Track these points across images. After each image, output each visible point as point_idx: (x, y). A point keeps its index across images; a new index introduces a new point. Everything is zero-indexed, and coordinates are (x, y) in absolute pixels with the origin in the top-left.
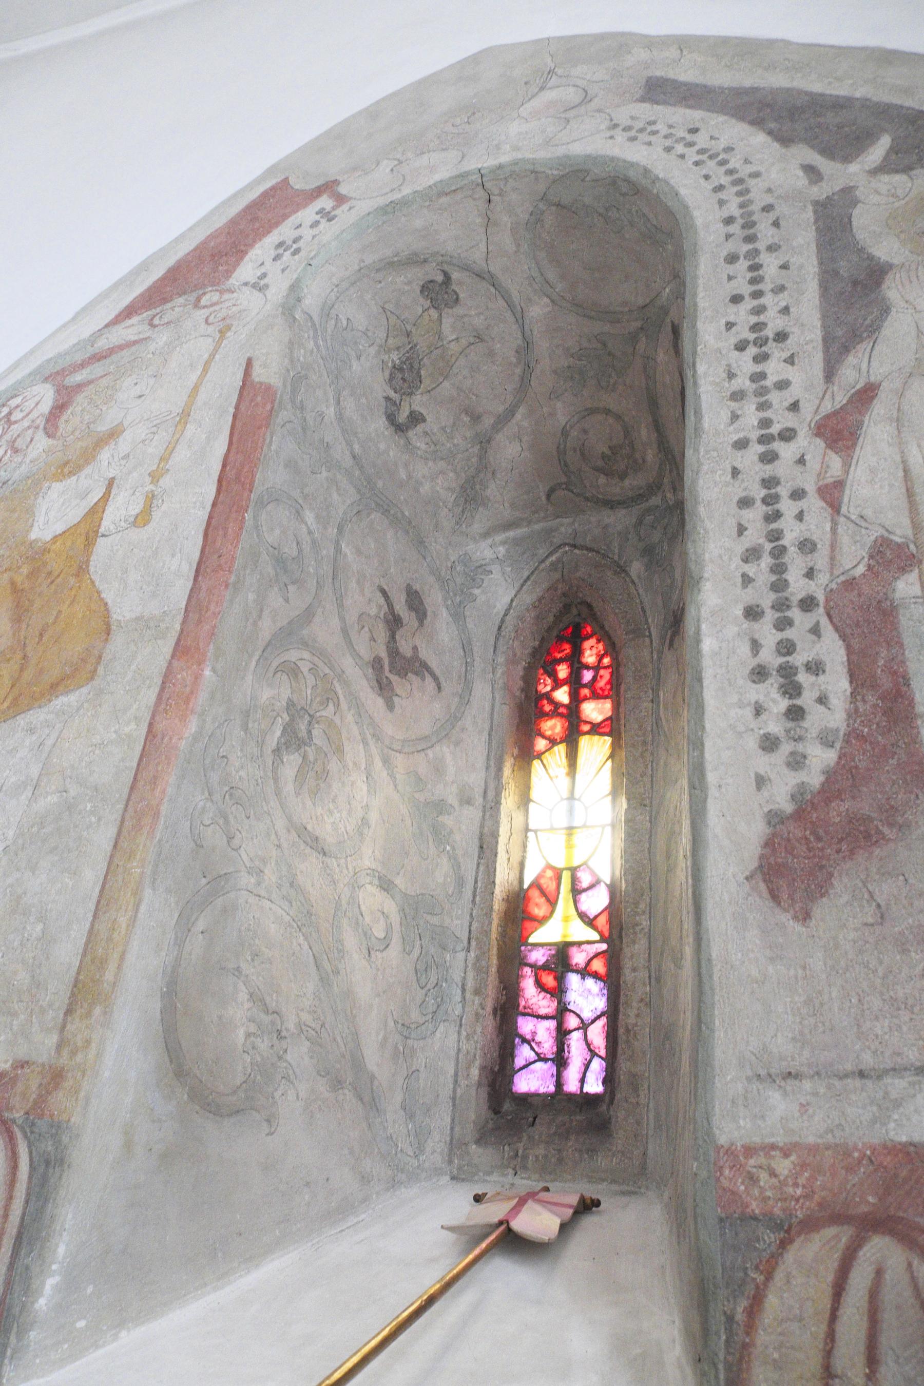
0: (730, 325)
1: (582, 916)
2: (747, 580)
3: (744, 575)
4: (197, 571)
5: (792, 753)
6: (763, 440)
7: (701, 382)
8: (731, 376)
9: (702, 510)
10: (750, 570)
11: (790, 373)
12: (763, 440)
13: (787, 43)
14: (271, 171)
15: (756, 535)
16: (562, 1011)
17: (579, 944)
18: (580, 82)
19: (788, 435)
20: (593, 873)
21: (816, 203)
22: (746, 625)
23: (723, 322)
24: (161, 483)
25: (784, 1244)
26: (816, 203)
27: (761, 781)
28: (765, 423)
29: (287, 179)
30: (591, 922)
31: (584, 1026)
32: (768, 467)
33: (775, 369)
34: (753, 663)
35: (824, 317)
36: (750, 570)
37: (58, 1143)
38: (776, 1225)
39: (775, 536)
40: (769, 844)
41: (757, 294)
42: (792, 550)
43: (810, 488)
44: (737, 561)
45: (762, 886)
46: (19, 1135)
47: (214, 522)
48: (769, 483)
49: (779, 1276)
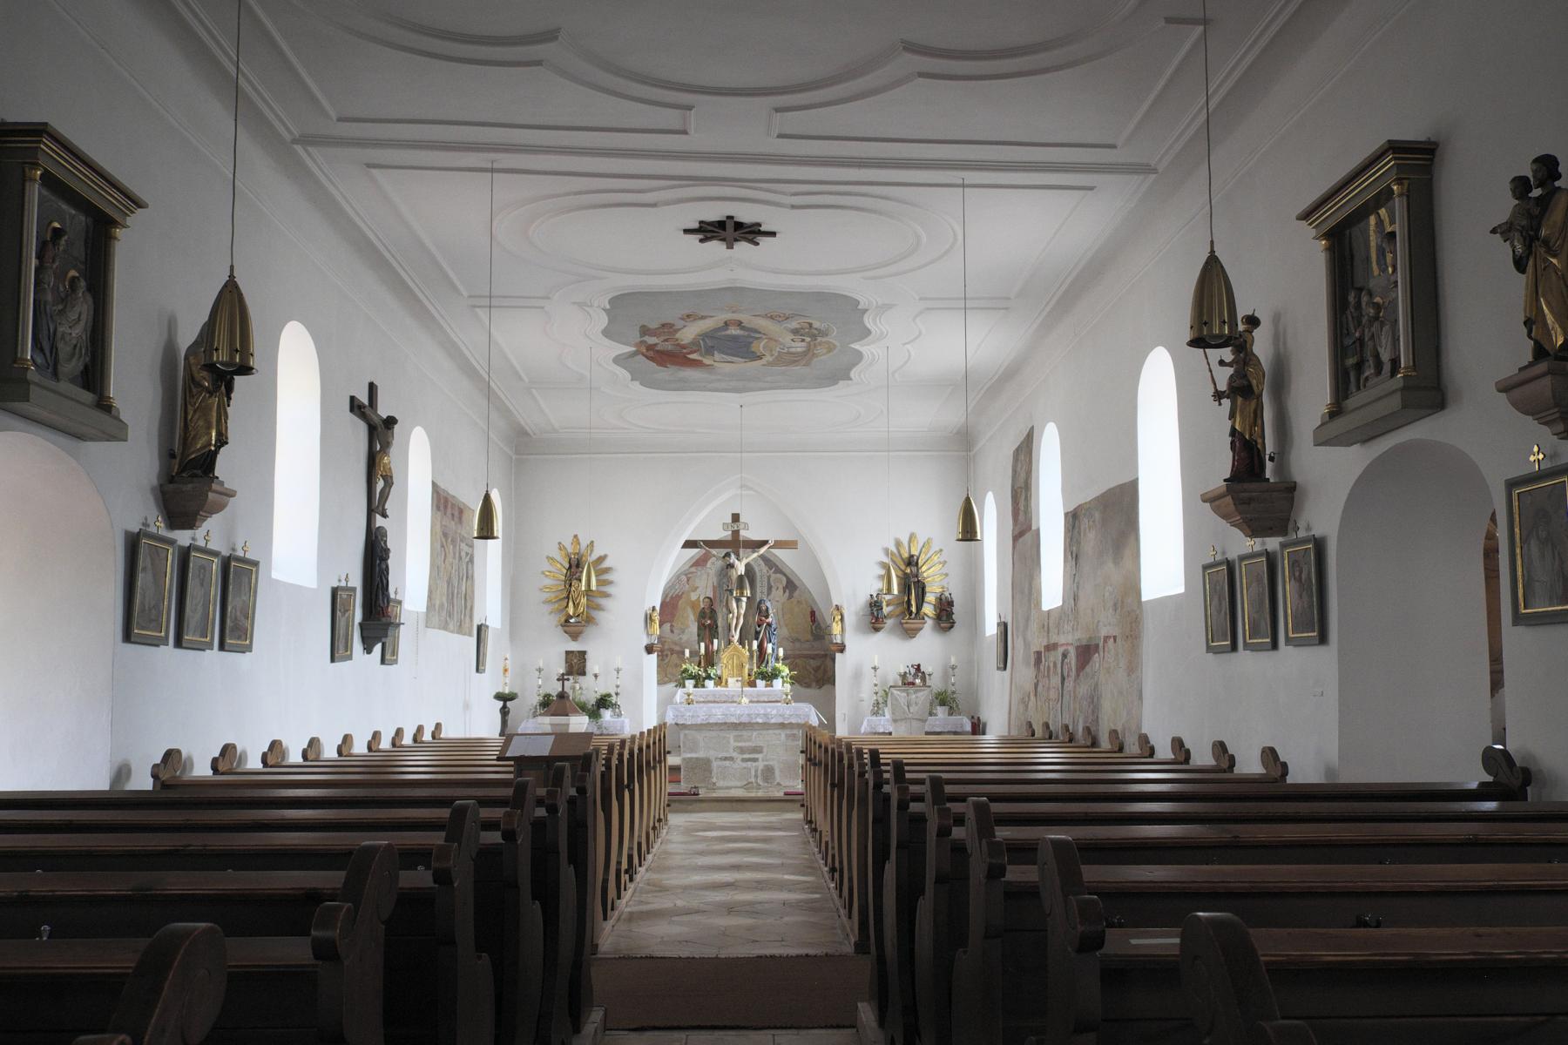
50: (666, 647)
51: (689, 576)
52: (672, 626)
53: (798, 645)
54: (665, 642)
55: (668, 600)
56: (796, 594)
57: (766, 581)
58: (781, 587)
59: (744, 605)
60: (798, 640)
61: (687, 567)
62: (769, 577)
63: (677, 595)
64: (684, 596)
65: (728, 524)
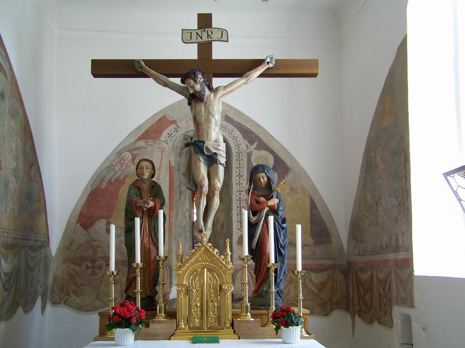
0: (236, 172)
2: (237, 210)
3: (237, 210)
4: (169, 198)
5: (241, 231)
6: (240, 191)
7: (233, 180)
8: (236, 180)
9: (233, 200)
10: (238, 209)
11: (243, 182)
12: (240, 191)
13: (245, 115)
14: (161, 111)
15: (238, 205)
19: (242, 191)
21: (247, 153)
22: (237, 216)
23: (235, 171)
24: (159, 181)
25: (238, 272)
26: (247, 153)
27: (238, 233)
28: (240, 189)
29: (165, 115)
32: (240, 196)
33: (241, 180)
34: (237, 220)
35: (247, 174)
36: (238, 209)
37: (171, 267)
38: (238, 270)
39: (240, 205)
40: (238, 239)
41: (240, 168)
42: (242, 207)
43: (244, 200)
44: (236, 208)
45: (238, 243)
46: (167, 267)
47: (170, 190)
48: (240, 198)
49: (238, 274)
50: (99, 255)
51: (135, 152)
54: (98, 247)
55: (104, 185)
57: (245, 159)
61: (133, 140)
62: (249, 155)
63: (117, 180)
65: (190, 31)
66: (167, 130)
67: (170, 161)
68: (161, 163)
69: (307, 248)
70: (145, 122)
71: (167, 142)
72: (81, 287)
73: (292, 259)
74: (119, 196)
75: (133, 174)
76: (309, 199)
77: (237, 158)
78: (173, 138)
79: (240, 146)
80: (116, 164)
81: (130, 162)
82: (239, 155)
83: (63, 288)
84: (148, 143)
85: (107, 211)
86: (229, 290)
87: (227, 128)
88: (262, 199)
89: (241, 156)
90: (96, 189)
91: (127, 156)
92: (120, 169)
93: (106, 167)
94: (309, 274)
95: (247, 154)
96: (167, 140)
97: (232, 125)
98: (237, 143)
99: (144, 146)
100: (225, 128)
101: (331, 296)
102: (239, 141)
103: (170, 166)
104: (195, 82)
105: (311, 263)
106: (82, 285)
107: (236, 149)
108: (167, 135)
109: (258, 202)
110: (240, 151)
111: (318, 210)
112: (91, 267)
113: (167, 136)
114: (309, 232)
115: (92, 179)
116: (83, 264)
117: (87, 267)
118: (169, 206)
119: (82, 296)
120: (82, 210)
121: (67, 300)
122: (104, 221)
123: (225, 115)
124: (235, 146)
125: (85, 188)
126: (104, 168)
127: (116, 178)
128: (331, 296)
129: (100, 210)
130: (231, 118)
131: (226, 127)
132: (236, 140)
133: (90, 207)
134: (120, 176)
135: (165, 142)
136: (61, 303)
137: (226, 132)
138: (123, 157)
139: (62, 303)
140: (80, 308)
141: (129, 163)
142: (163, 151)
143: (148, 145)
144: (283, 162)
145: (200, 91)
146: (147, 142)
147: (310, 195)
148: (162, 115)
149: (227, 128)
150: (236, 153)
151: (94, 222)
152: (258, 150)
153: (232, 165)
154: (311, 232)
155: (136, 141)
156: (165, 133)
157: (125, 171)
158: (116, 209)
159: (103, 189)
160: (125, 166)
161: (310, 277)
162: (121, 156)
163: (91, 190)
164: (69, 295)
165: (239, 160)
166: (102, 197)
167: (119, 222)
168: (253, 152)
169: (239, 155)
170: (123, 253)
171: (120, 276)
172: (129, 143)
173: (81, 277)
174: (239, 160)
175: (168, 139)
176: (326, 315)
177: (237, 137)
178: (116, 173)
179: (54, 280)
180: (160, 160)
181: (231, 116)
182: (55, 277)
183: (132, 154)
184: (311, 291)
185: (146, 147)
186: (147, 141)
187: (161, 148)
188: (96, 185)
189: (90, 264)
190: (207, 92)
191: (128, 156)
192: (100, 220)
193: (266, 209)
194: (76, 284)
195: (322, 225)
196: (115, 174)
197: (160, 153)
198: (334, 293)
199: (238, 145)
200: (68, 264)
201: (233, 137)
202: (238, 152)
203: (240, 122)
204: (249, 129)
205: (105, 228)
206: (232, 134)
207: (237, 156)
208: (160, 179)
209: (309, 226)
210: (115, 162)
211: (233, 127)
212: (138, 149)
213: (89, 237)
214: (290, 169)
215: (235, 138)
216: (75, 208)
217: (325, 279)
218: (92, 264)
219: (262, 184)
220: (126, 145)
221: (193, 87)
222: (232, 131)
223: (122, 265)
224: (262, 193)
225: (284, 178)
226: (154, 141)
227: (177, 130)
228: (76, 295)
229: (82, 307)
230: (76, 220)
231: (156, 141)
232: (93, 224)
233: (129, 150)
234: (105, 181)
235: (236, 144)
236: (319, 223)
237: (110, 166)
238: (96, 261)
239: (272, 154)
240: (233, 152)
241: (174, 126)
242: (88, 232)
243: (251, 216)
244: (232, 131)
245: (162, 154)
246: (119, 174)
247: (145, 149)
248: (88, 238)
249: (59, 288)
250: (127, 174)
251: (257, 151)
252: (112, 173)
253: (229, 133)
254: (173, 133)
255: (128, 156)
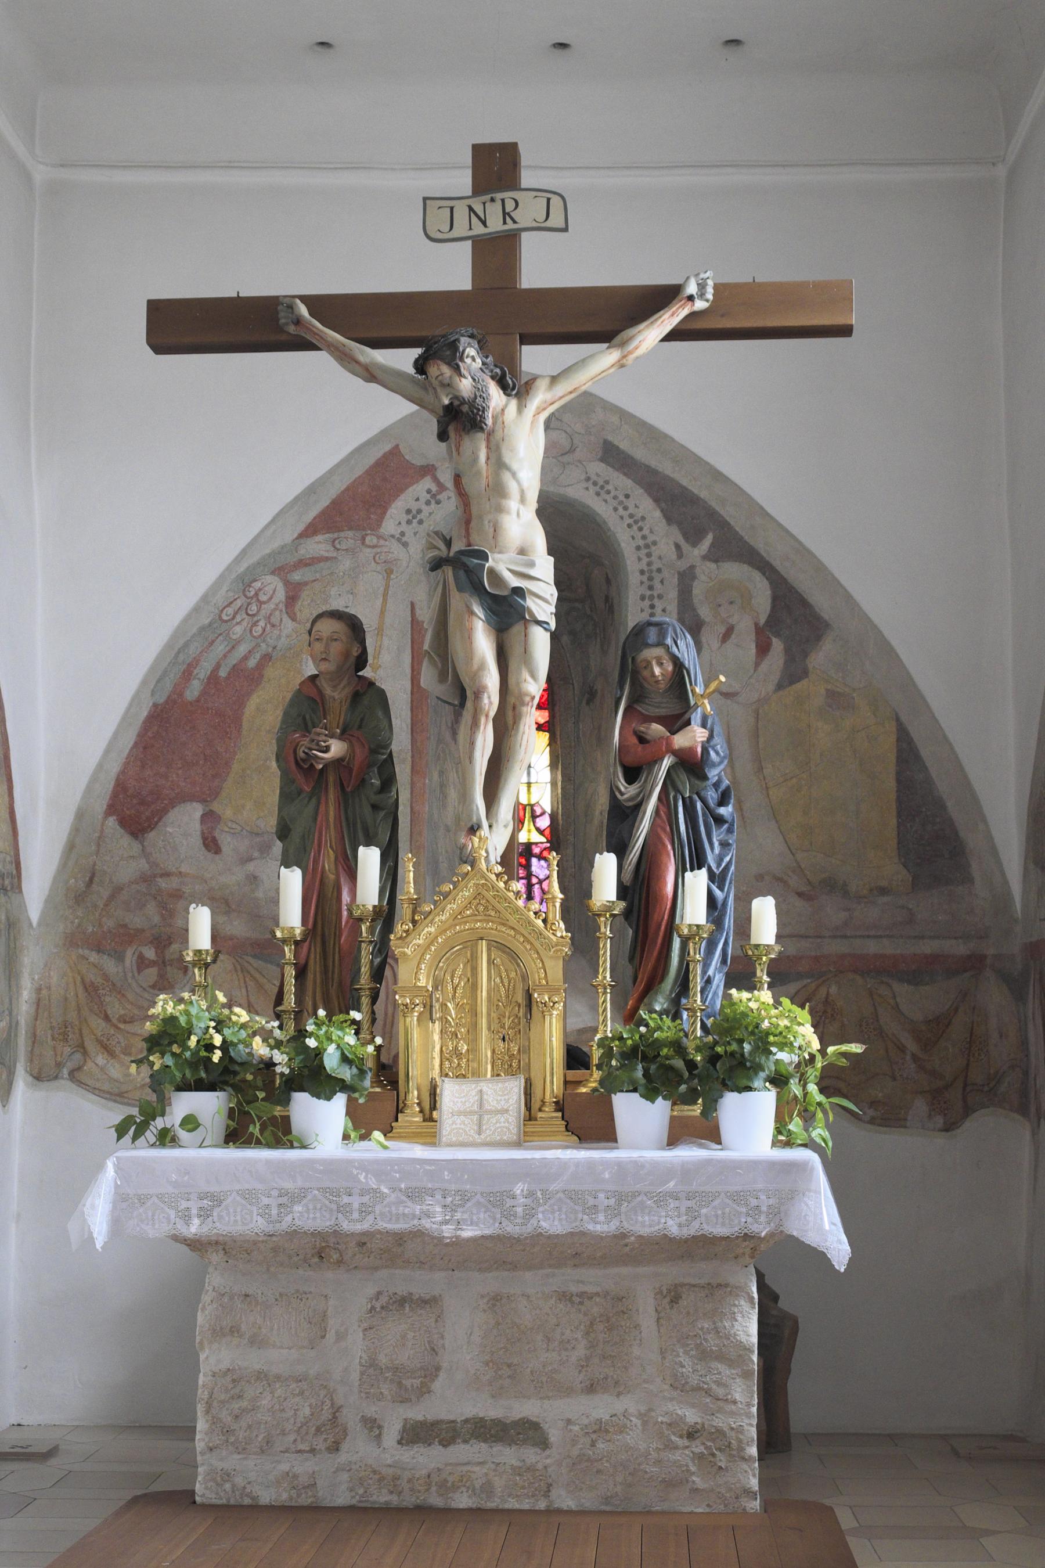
1: (538, 829)
13: (673, 440)
14: (384, 433)
16: (529, 876)
17: (536, 844)
18: (568, 430)
20: (542, 808)
24: (378, 672)
26: (679, 573)
29: (397, 446)
30: (541, 832)
31: (540, 882)
47: (414, 704)
51: (296, 577)
52: (210, 818)
53: (833, 912)
55: (194, 690)
56: (820, 658)
57: (673, 594)
58: (745, 626)
59: (541, 644)
60: (831, 885)
61: (289, 536)
62: (686, 579)
63: (237, 670)
64: (270, 672)
66: (402, 497)
67: (412, 605)
68: (382, 612)
69: (885, 899)
70: (331, 472)
71: (404, 539)
72: (122, 1026)
73: (835, 937)
74: (245, 725)
75: (290, 648)
76: (894, 729)
77: (644, 590)
78: (425, 525)
79: (653, 548)
80: (234, 618)
81: (281, 611)
82: (650, 579)
83: (66, 1028)
84: (339, 543)
85: (204, 775)
86: (554, 1003)
87: (610, 487)
88: (657, 729)
89: (656, 583)
90: (166, 702)
91: (269, 589)
92: (249, 635)
93: (202, 629)
94: (891, 987)
95: (676, 576)
96: (403, 534)
97: (625, 474)
98: (644, 537)
99: (326, 554)
100: (602, 487)
101: (968, 1065)
102: (651, 532)
103: (412, 620)
104: (457, 369)
105: (899, 952)
106: (125, 1022)
107: (640, 559)
108: (404, 515)
109: (642, 740)
110: (654, 567)
111: (924, 768)
112: (153, 963)
113: (405, 518)
114: (894, 843)
115: (153, 668)
116: (129, 953)
117: (142, 963)
118: (410, 759)
119: (124, 1054)
120: (123, 772)
121: (79, 1069)
122: (195, 811)
123: (602, 441)
124: (638, 548)
125: (133, 700)
126: (194, 630)
127: (234, 666)
128: (968, 1065)
129: (180, 772)
130: (623, 452)
131: (607, 482)
132: (640, 529)
133: (150, 764)
134: (246, 658)
135: (399, 540)
136: (60, 1075)
137: (606, 501)
138: (256, 594)
139: (62, 1078)
140: (121, 1095)
141: (277, 613)
142: (389, 572)
143: (338, 550)
144: (804, 603)
145: (473, 396)
146: (337, 542)
147: (897, 714)
148: (388, 447)
149: (610, 487)
150: (638, 574)
151: (164, 811)
152: (716, 561)
153: (626, 616)
154: (899, 843)
155: (301, 536)
156: (396, 511)
157: (264, 641)
158: (236, 767)
159: (191, 703)
160: (262, 623)
161: (894, 997)
162: (251, 589)
163: (151, 704)
164: (85, 1053)
165: (651, 598)
166: (188, 728)
167: (245, 813)
168: (698, 571)
169: (650, 579)
170: (260, 917)
171: (247, 991)
172: (276, 544)
173: (123, 995)
174: (651, 598)
175: (409, 530)
176: (949, 1128)
177: (643, 518)
178: (233, 647)
179: (38, 1003)
180: (379, 602)
181: (624, 445)
182: (39, 990)
183: (287, 583)
184: (898, 1047)
185: (336, 558)
186: (336, 535)
187: (385, 562)
188: (168, 686)
189: (150, 953)
190: (496, 397)
191: (274, 591)
192: (182, 805)
193: (667, 762)
194: (107, 1018)
195: (938, 820)
196: (229, 651)
197: (381, 577)
198: (976, 1055)
199: (647, 546)
200: (80, 951)
201: (631, 516)
202: (646, 568)
203: (653, 463)
204: (687, 489)
205: (199, 833)
206: (626, 508)
207: (642, 583)
208: (380, 666)
209: (893, 822)
210: (230, 611)
211: (629, 483)
212: (307, 565)
213: (148, 863)
214: (827, 625)
215: (636, 522)
216: (100, 766)
217: (947, 1007)
218: (156, 953)
219: (657, 682)
220: (268, 551)
221: (448, 385)
222: (627, 496)
223: (255, 956)
224: (657, 710)
225: (806, 656)
226: (359, 534)
227: (438, 497)
228: (108, 1052)
229: (126, 1092)
230: (105, 807)
231: (367, 535)
232: (160, 819)
233: (275, 570)
234: (197, 674)
235: (641, 543)
236: (928, 813)
237: (215, 626)
238: (170, 944)
239: (764, 574)
240: (629, 568)
241: (427, 483)
242: (143, 846)
243: (622, 784)
244: (627, 496)
245: (388, 578)
246: (242, 649)
247: (328, 564)
248: (143, 865)
249: (52, 1028)
250: (270, 650)
251: (713, 566)
252: (220, 648)
253: (615, 503)
254: (424, 507)
255: (274, 588)
